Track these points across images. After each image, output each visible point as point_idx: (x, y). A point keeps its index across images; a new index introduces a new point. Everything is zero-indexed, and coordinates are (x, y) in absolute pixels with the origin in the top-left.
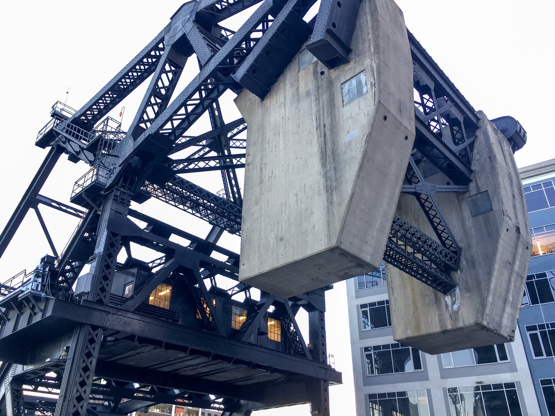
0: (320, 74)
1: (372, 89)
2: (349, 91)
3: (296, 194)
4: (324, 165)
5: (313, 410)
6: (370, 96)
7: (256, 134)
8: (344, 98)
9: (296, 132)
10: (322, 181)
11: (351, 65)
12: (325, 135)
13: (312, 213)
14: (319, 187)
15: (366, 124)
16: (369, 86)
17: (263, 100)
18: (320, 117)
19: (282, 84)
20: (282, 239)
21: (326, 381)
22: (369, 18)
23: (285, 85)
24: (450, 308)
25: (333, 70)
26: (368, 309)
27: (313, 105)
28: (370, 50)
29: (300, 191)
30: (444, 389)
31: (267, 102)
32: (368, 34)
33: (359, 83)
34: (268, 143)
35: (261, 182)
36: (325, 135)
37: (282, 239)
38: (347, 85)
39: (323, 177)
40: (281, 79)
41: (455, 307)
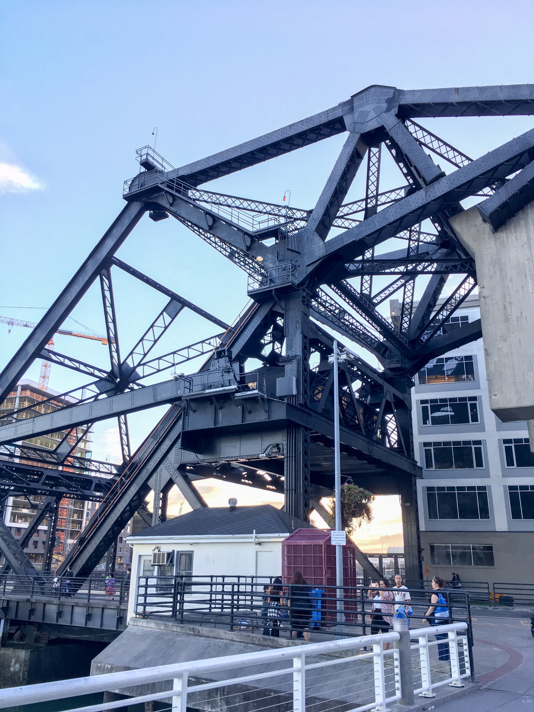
5: (404, 501)
7: (491, 268)
17: (496, 232)
19: (522, 222)
21: (415, 476)
23: (527, 224)
26: (429, 405)
31: (502, 235)
34: (511, 280)
35: (507, 320)
40: (520, 215)
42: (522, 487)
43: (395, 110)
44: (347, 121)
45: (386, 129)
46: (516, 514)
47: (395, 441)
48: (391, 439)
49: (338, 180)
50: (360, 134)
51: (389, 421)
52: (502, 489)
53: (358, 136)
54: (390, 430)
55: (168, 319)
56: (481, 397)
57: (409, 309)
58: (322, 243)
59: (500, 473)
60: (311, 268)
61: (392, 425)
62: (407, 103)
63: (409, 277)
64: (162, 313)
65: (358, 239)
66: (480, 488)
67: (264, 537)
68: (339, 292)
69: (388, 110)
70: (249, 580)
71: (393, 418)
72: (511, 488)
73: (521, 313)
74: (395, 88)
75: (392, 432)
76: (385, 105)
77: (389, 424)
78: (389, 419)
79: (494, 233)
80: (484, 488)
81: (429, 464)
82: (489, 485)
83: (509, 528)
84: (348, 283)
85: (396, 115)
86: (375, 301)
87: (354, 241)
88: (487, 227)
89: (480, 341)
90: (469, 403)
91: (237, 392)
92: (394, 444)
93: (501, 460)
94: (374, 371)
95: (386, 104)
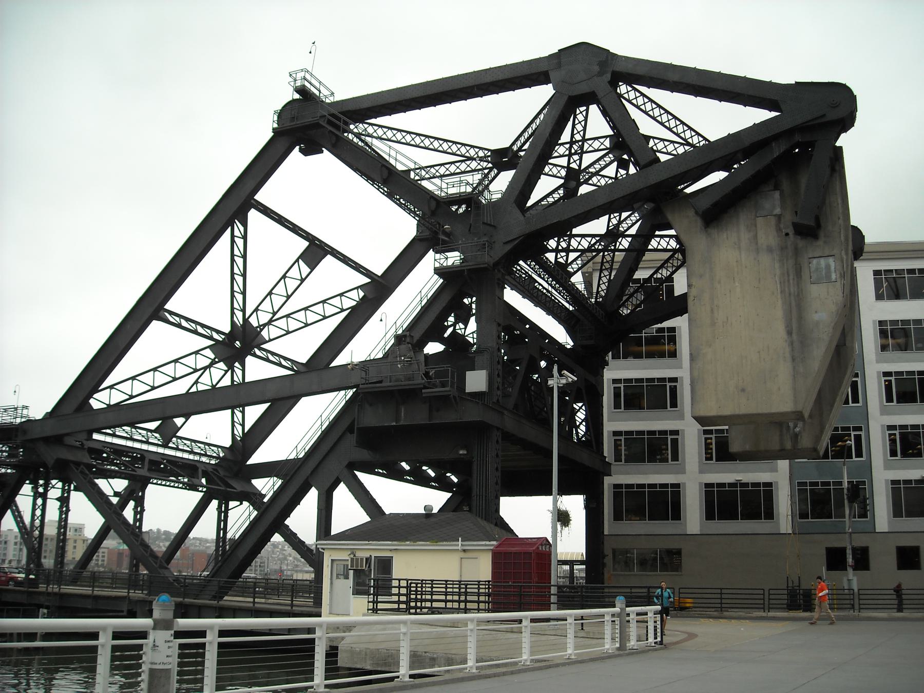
0: (784, 234)
1: (841, 280)
2: (817, 269)
3: (759, 352)
4: (790, 333)
6: (838, 284)
8: (812, 275)
9: (756, 286)
10: (788, 350)
11: (820, 242)
12: (790, 304)
13: (777, 376)
14: (784, 353)
15: (834, 311)
16: (838, 275)
18: (784, 282)
20: (743, 390)
22: (840, 201)
24: (791, 431)
25: (799, 237)
26: (622, 386)
27: (777, 265)
28: (840, 237)
29: (763, 350)
30: (700, 484)
32: (839, 219)
33: (828, 267)
34: (719, 282)
35: (713, 324)
36: (790, 304)
37: (743, 390)
38: (815, 261)
39: (789, 345)
41: (797, 429)
42: (720, 485)
43: (608, 76)
44: (552, 75)
45: (597, 96)
47: (583, 433)
48: (579, 431)
49: (542, 146)
50: (568, 96)
51: (579, 410)
54: (578, 420)
55: (305, 269)
56: (682, 378)
57: (604, 270)
58: (522, 218)
59: (696, 469)
60: (508, 247)
61: (581, 415)
62: (621, 70)
63: (610, 240)
64: (297, 261)
65: (563, 219)
66: (673, 485)
67: (471, 545)
68: (533, 263)
69: (601, 74)
71: (584, 408)
72: (707, 485)
73: (727, 319)
74: (609, 51)
75: (581, 423)
76: (596, 68)
77: (579, 414)
78: (578, 408)
79: (705, 228)
80: (678, 486)
81: (618, 459)
82: (683, 482)
83: (701, 530)
84: (547, 258)
85: (609, 82)
86: (570, 269)
87: (559, 221)
88: (699, 222)
89: (686, 316)
90: (668, 384)
91: (425, 388)
92: (582, 437)
94: (561, 347)
95: (598, 67)
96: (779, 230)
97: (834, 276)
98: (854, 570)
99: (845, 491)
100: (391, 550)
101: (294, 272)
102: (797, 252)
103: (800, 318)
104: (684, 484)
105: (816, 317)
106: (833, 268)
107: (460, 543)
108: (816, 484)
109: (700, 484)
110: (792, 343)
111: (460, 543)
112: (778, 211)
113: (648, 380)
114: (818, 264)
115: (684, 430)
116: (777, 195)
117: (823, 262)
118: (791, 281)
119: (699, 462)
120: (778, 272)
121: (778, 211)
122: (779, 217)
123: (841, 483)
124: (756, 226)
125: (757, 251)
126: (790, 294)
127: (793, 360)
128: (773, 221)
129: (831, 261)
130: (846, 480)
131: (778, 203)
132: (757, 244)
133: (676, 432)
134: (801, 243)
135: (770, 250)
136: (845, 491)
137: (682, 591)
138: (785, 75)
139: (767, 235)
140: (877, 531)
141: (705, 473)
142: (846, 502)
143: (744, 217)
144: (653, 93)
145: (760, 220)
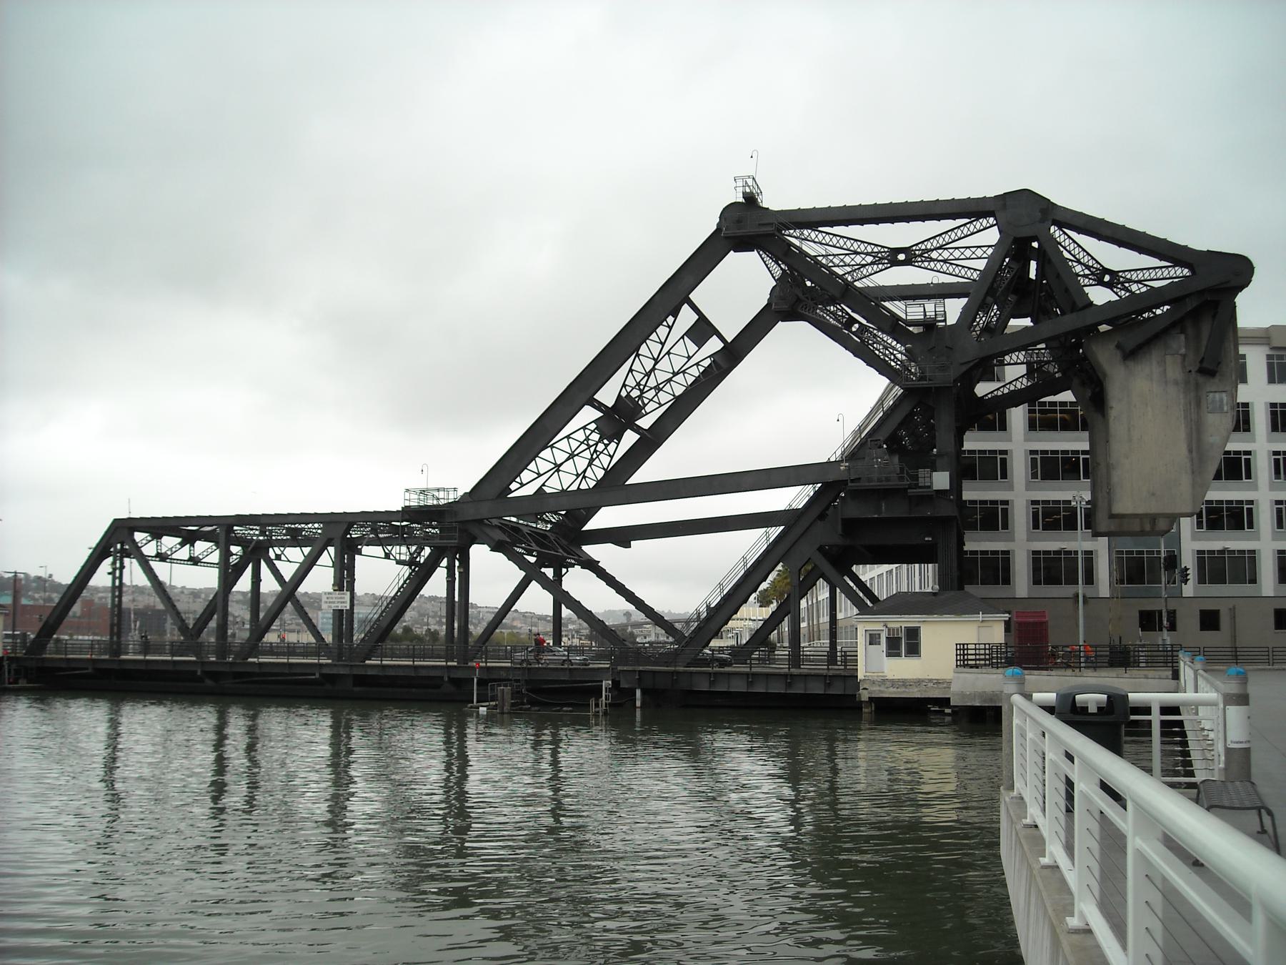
2: (1213, 401)
3: (1166, 465)
4: (1190, 451)
11: (1216, 380)
20: (1153, 494)
22: (1232, 347)
27: (1182, 396)
30: (1028, 550)
31: (1131, 364)
33: (1221, 401)
37: (1153, 494)
42: (1046, 552)
46: (1036, 582)
52: (1026, 554)
53: (1011, 239)
55: (692, 347)
59: (1025, 537)
60: (964, 368)
64: (682, 337)
67: (989, 617)
70: (973, 647)
72: (1034, 552)
76: (1039, 215)
80: (1007, 552)
83: (1029, 593)
88: (1119, 354)
90: (999, 457)
91: (910, 488)
93: (1028, 523)
96: (1184, 367)
97: (1225, 408)
98: (1168, 631)
99: (1162, 561)
100: (919, 622)
101: (680, 349)
102: (1197, 387)
103: (1199, 440)
104: (1014, 551)
105: (1211, 440)
106: (1225, 401)
107: (981, 615)
108: (1132, 552)
109: (1028, 550)
110: (1192, 460)
111: (981, 615)
112: (1183, 351)
113: (980, 452)
114: (1214, 397)
115: (1013, 501)
116: (1182, 337)
117: (1217, 395)
118: (1193, 410)
119: (1027, 531)
120: (1182, 401)
121: (1183, 351)
122: (1184, 356)
123: (1159, 552)
124: (1165, 363)
125: (1166, 383)
126: (1191, 420)
127: (1193, 472)
128: (1179, 359)
129: (1224, 395)
130: (1163, 550)
131: (1183, 344)
132: (1165, 377)
133: (1006, 502)
134: (1201, 379)
135: (1176, 383)
136: (1162, 561)
137: (1275, 649)
138: (1200, 243)
139: (1174, 371)
140: (1184, 596)
141: (1032, 541)
142: (1163, 570)
143: (1155, 354)
144: (1082, 239)
145: (1168, 358)
